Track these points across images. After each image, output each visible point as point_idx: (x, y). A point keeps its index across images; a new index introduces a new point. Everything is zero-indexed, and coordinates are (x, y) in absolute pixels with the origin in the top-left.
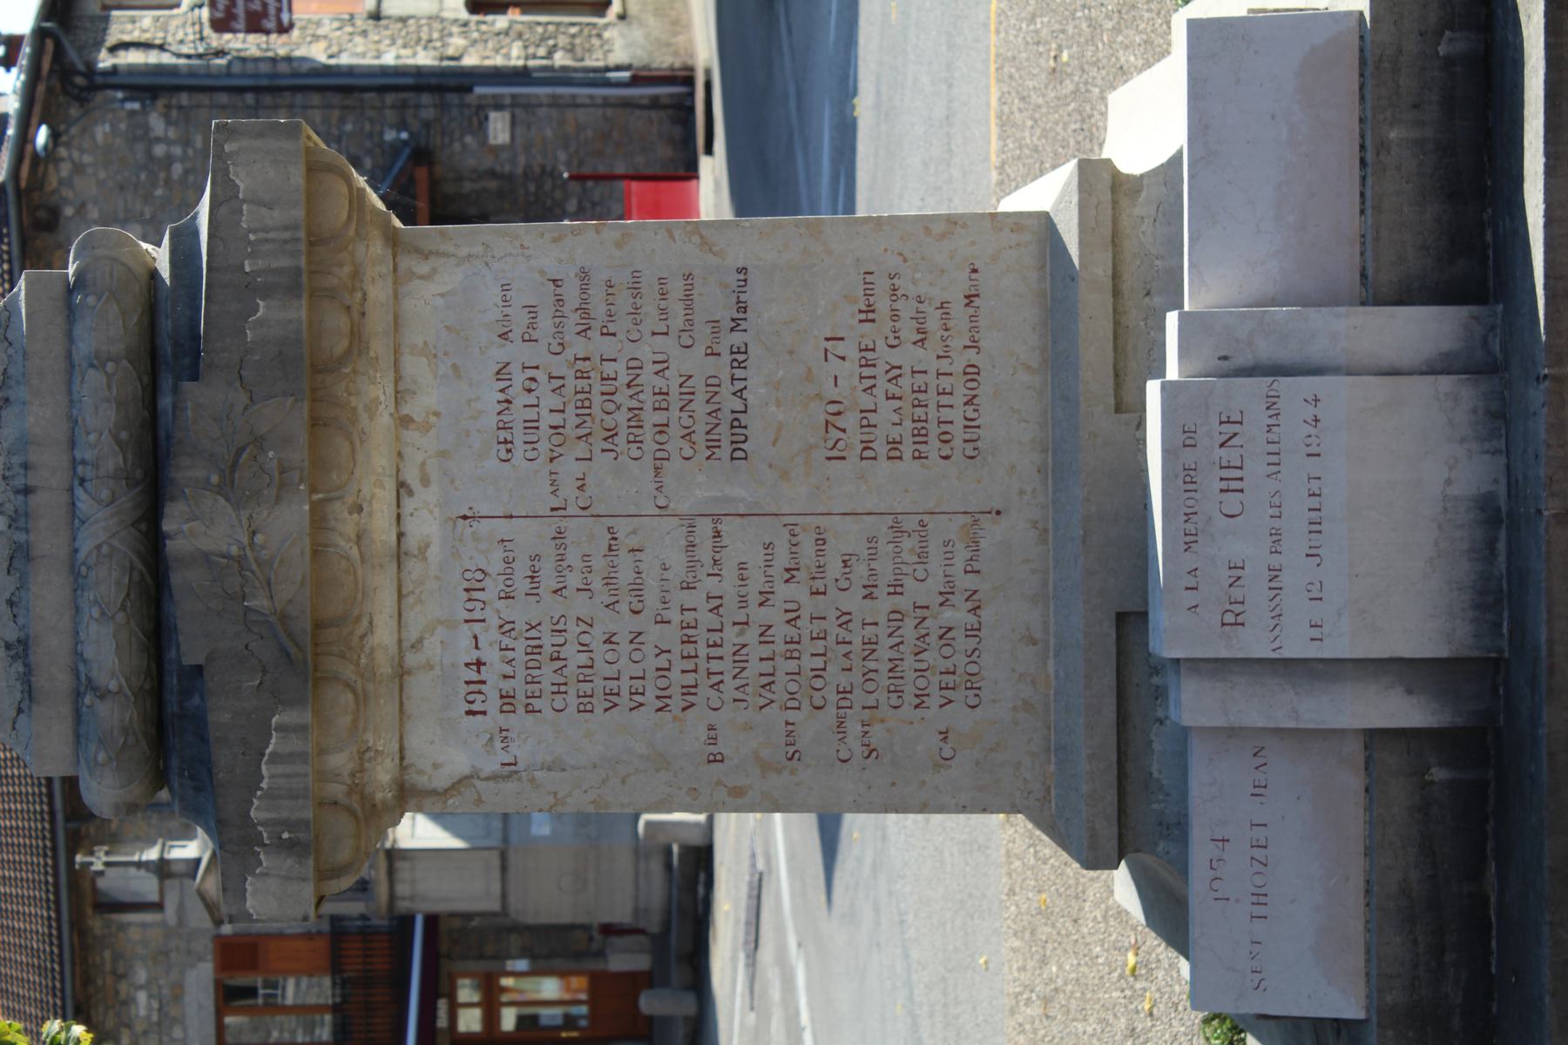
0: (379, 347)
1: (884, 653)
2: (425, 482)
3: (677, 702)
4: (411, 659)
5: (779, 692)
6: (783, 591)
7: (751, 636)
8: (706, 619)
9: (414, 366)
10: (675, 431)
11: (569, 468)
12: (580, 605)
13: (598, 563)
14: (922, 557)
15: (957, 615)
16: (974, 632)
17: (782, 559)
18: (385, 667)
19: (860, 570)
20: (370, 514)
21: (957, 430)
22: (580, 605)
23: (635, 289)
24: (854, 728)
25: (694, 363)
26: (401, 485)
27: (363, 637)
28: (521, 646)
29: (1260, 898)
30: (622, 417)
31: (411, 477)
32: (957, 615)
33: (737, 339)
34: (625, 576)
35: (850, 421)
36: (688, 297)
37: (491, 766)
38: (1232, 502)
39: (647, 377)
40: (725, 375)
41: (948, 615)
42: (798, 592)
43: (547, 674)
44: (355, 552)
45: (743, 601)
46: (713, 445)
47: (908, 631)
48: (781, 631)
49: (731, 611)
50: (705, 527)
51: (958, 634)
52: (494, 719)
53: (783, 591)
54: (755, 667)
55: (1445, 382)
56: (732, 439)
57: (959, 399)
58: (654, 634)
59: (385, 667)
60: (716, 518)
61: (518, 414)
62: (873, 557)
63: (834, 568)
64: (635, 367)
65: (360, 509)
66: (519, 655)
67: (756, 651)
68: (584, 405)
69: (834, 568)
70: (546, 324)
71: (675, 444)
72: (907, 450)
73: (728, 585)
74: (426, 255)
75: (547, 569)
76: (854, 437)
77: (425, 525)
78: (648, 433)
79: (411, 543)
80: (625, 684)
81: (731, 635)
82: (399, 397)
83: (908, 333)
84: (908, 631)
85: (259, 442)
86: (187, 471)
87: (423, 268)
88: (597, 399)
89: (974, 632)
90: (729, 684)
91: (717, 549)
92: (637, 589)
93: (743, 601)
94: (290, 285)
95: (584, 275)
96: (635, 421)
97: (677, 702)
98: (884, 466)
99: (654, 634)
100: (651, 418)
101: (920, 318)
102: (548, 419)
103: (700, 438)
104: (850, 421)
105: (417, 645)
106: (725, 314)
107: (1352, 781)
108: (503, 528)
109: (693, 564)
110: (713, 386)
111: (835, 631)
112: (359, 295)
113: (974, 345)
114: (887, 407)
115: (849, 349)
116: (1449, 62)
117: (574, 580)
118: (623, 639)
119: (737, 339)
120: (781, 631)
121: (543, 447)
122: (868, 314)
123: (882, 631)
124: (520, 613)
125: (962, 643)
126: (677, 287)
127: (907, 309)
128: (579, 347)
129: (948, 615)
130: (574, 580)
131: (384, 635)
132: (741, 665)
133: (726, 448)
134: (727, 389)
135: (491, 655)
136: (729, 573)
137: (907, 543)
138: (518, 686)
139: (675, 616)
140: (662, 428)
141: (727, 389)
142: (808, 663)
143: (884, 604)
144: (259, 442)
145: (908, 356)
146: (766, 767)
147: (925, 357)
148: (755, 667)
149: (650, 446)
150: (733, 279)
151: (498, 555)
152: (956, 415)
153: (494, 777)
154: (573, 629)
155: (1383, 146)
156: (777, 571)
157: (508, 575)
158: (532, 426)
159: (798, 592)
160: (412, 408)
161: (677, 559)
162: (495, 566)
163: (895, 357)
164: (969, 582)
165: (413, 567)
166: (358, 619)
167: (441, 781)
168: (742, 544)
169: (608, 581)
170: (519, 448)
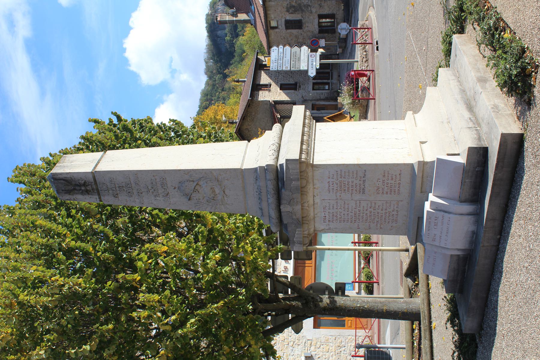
0: (310, 181)
5: (368, 221)
6: (369, 209)
7: (365, 214)
8: (358, 212)
10: (354, 190)
11: (338, 194)
12: (340, 210)
13: (343, 205)
14: (390, 206)
15: (395, 213)
17: (369, 205)
18: (312, 218)
19: (381, 207)
22: (340, 210)
23: (349, 172)
25: (358, 182)
26: (314, 196)
29: (434, 264)
30: (346, 188)
31: (315, 195)
33: (364, 179)
34: (346, 207)
35: (381, 189)
36: (357, 174)
38: (435, 227)
39: (350, 183)
41: (393, 213)
43: (335, 218)
45: (363, 211)
46: (360, 192)
47: (387, 214)
48: (369, 214)
49: (362, 211)
50: (358, 202)
52: (327, 223)
53: (369, 209)
54: (365, 218)
55: (470, 217)
56: (363, 191)
57: (397, 187)
58: (350, 214)
61: (331, 188)
63: (377, 207)
64: (348, 182)
67: (365, 216)
68: (341, 187)
69: (377, 207)
70: (335, 177)
71: (354, 191)
72: (389, 193)
73: (361, 209)
76: (381, 192)
77: (317, 200)
78: (350, 190)
79: (315, 202)
81: (361, 214)
82: (313, 185)
83: (390, 178)
85: (294, 199)
86: (283, 202)
87: (317, 169)
88: (343, 186)
92: (348, 209)
93: (363, 211)
94: (298, 180)
95: (341, 170)
96: (348, 188)
97: (353, 222)
99: (350, 214)
100: (350, 188)
102: (335, 188)
103: (358, 191)
104: (381, 189)
106: (362, 175)
107: (448, 259)
108: (329, 201)
110: (360, 185)
111: (376, 214)
113: (400, 180)
115: (381, 181)
116: (477, 171)
117: (339, 207)
119: (364, 179)
121: (335, 192)
122: (384, 176)
124: (331, 211)
126: (355, 172)
127: (390, 176)
128: (340, 179)
129: (393, 213)
130: (339, 207)
132: (363, 218)
135: (327, 216)
136: (362, 207)
138: (331, 219)
140: (352, 190)
143: (384, 211)
144: (294, 199)
145: (389, 181)
146: (366, 229)
147: (393, 182)
149: (350, 192)
150: (364, 171)
154: (339, 213)
155: (465, 182)
156: (369, 207)
159: (372, 210)
160: (316, 186)
161: (354, 206)
163: (388, 182)
164: (397, 209)
165: (316, 206)
168: (364, 204)
170: (331, 192)
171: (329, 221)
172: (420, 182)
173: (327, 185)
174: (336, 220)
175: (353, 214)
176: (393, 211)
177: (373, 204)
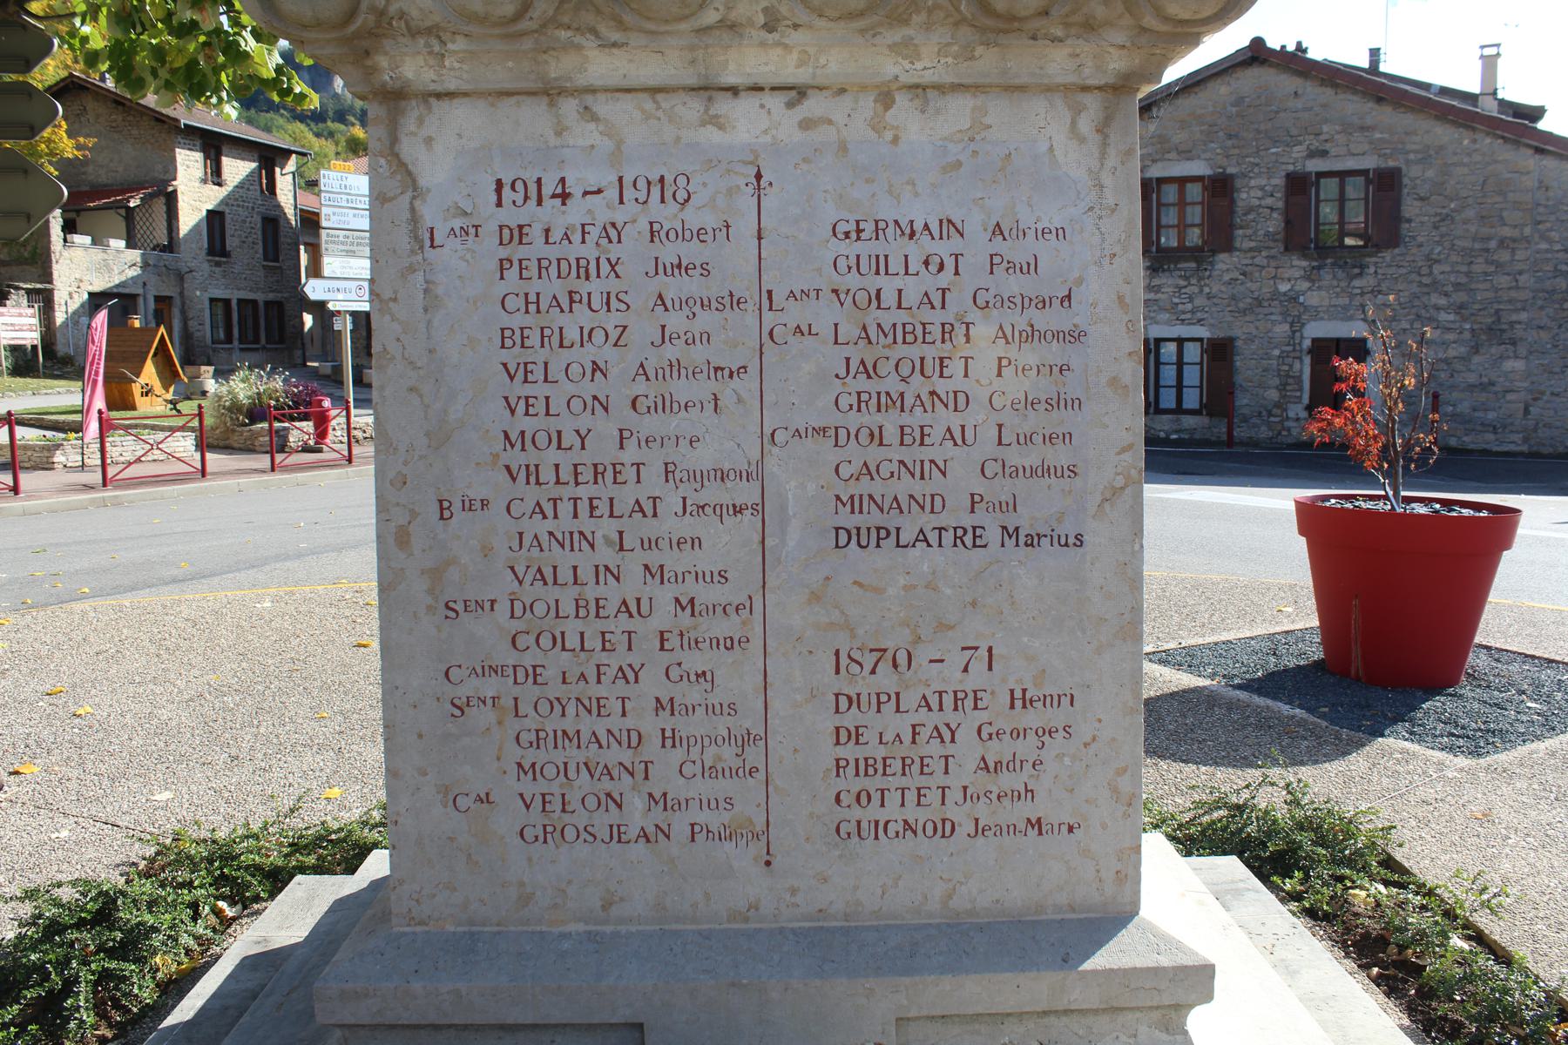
0: (987, 62)
1: (587, 724)
2: (806, 124)
3: (516, 458)
4: (569, 106)
5: (529, 592)
6: (664, 596)
7: (605, 555)
8: (626, 496)
9: (958, 112)
10: (874, 454)
11: (824, 314)
12: (643, 330)
13: (699, 354)
14: (712, 772)
15: (637, 814)
16: (617, 834)
18: (558, 67)
19: (692, 694)
20: (763, 44)
21: (873, 812)
22: (643, 330)
24: (490, 687)
25: (962, 479)
27: (594, 32)
28: (589, 252)
30: (892, 385)
31: (814, 106)
32: (637, 814)
33: (993, 535)
34: (682, 389)
35: (886, 680)
36: (1046, 471)
37: (430, 214)
39: (944, 418)
40: (945, 519)
41: (636, 803)
42: (664, 616)
43: (552, 287)
44: (711, 17)
47: (616, 755)
48: (612, 593)
49: (637, 528)
50: (746, 493)
51: (614, 815)
52: (492, 218)
53: (664, 596)
54: (565, 560)
56: (862, 529)
58: (604, 427)
59: (558, 67)
60: (759, 509)
61: (895, 248)
62: (710, 710)
63: (695, 661)
65: (769, 27)
66: (576, 250)
67: (585, 561)
68: (906, 334)
69: (695, 661)
70: (1014, 285)
71: (856, 456)
72: (849, 751)
73: (670, 524)
74: (1102, 129)
75: (689, 285)
76: (864, 685)
77: (749, 123)
78: (871, 419)
80: (540, 390)
81: (607, 527)
83: (997, 750)
84: (616, 755)
87: (1086, 125)
88: (915, 351)
89: (617, 834)
90: (542, 527)
91: (719, 510)
92: (664, 405)
93: (650, 544)
95: (1076, 336)
97: (516, 458)
98: (828, 722)
99: (604, 427)
100: (890, 423)
101: (1015, 764)
102: (889, 286)
103: (865, 486)
104: (886, 680)
105: (588, 114)
106: (1025, 519)
108: (745, 227)
109: (698, 478)
110: (932, 504)
111: (614, 662)
112: (1059, 33)
113: (979, 830)
114: (903, 725)
115: (978, 676)
117: (676, 321)
118: (599, 386)
119: (993, 535)
120: (612, 593)
121: (853, 280)
123: (615, 722)
124: (633, 251)
125: (602, 821)
126: (1060, 456)
127: (1026, 748)
129: (636, 803)
130: (676, 321)
131: (600, 66)
133: (851, 521)
134: (928, 521)
135: (576, 212)
136: (688, 527)
137: (728, 753)
138: (536, 247)
139: (630, 454)
141: (928, 521)
142: (572, 628)
143: (650, 725)
145: (967, 750)
146: (436, 575)
147: (965, 772)
148: (565, 560)
149: (854, 420)
150: (1068, 529)
151: (710, 221)
152: (892, 811)
153: (414, 218)
154: (612, 321)
156: (690, 588)
157: (682, 234)
158: (881, 265)
159: (664, 616)
160: (903, 111)
161: (703, 458)
162: (694, 217)
163: (966, 735)
164: (680, 828)
165: (691, 108)
166: (621, 25)
167: (409, 148)
168: (727, 542)
169: (675, 367)
170: (851, 248)
171: (520, 233)
172: (1008, 1003)
173: (919, 212)
174: (531, 303)
175: (603, 449)
176: (660, 801)
177: (722, 627)
